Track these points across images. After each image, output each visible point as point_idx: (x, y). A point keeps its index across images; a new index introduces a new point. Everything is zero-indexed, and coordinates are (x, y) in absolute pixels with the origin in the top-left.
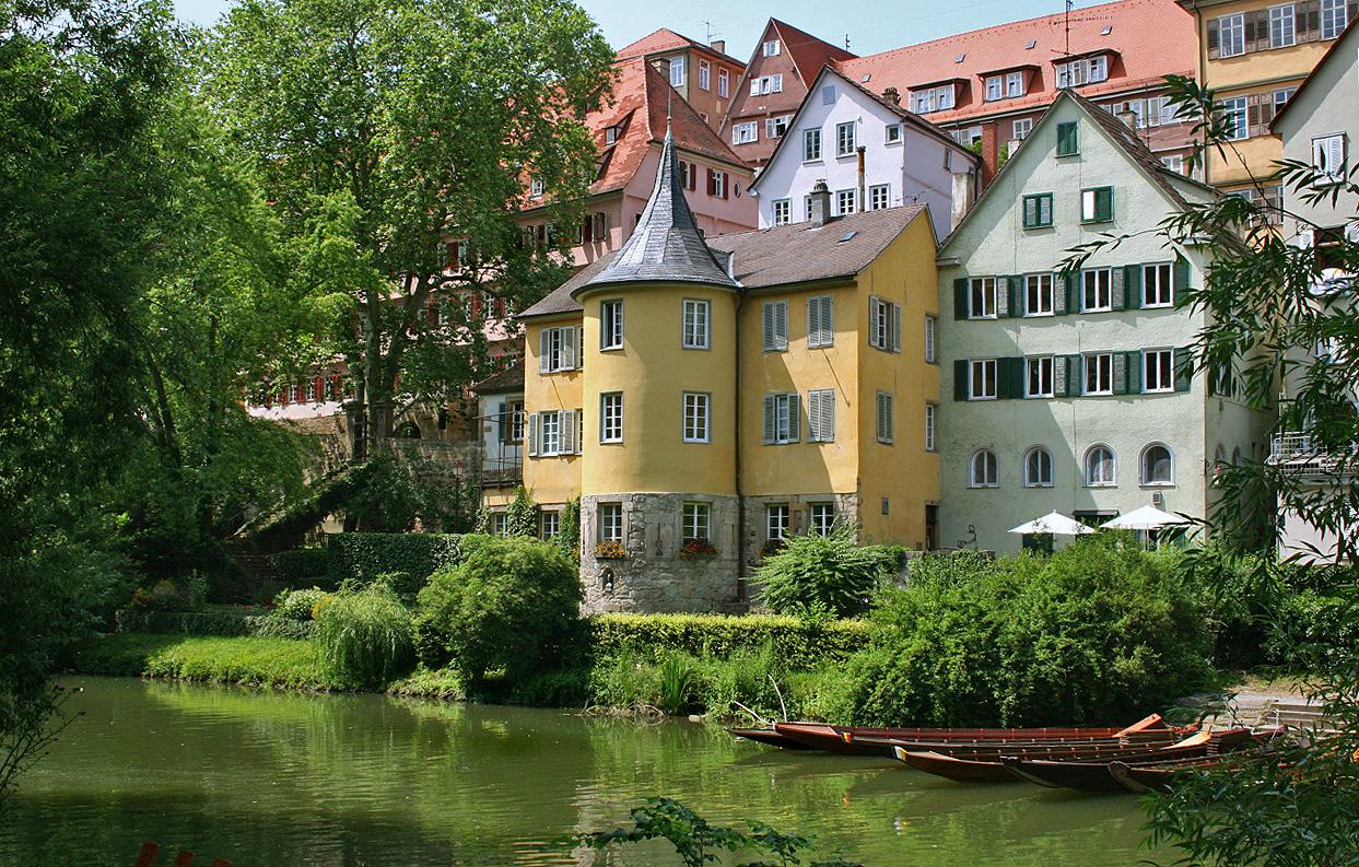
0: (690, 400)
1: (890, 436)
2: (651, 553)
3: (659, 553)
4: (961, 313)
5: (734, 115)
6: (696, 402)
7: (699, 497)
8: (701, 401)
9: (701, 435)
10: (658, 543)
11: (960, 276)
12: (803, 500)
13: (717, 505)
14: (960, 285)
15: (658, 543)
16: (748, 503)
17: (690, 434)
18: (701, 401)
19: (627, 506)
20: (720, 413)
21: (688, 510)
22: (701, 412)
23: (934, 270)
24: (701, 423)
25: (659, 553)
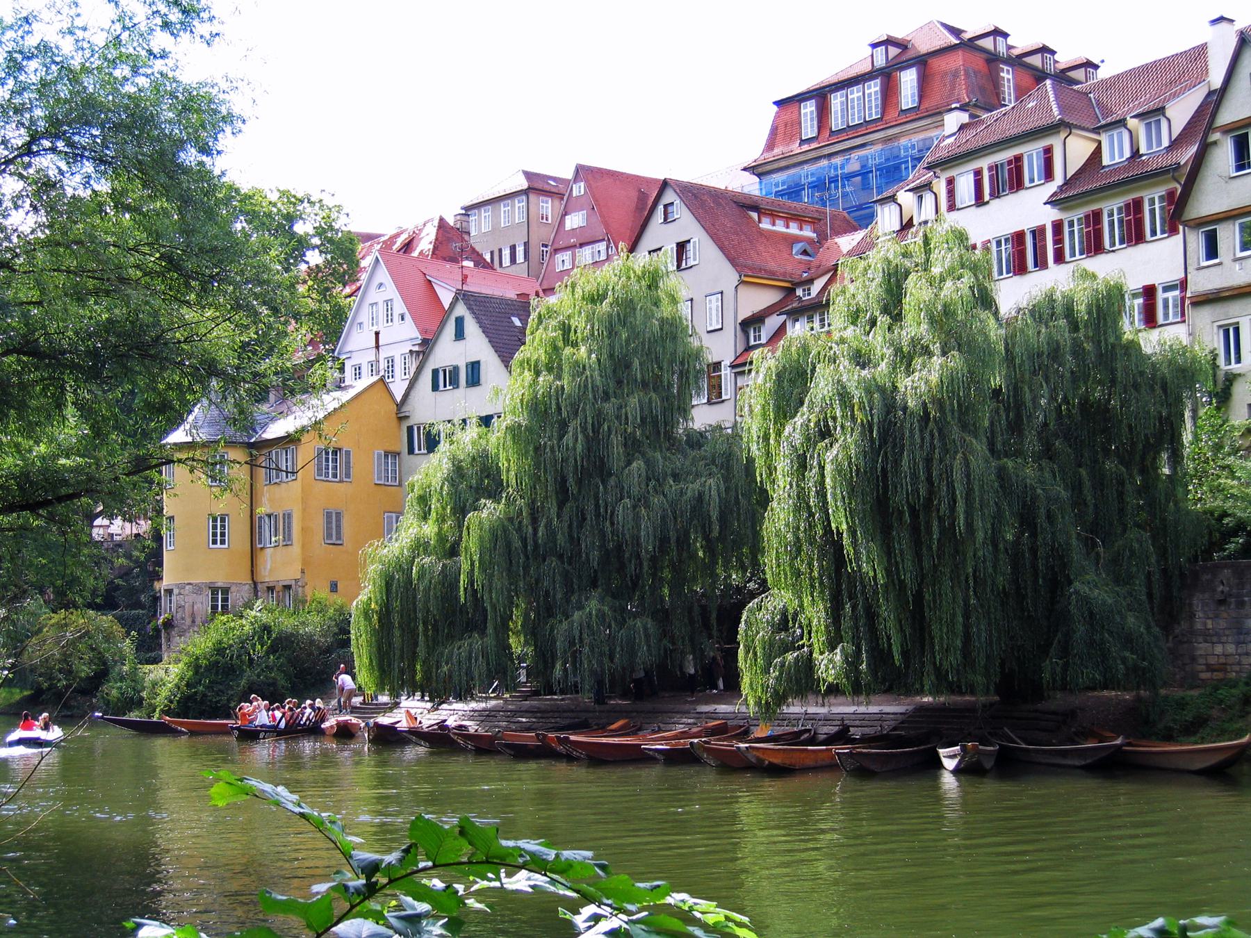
0: (215, 520)
1: (339, 538)
2: (188, 621)
3: (193, 622)
4: (411, 451)
5: (556, 246)
6: (218, 522)
7: (219, 584)
8: (223, 520)
9: (223, 542)
10: (193, 615)
11: (410, 422)
12: (281, 584)
13: (233, 589)
14: (410, 429)
15: (193, 615)
16: (259, 587)
17: (215, 542)
18: (223, 520)
19: (176, 591)
20: (238, 531)
21: (214, 591)
22: (223, 526)
23: (395, 420)
24: (223, 534)
25: (193, 622)
